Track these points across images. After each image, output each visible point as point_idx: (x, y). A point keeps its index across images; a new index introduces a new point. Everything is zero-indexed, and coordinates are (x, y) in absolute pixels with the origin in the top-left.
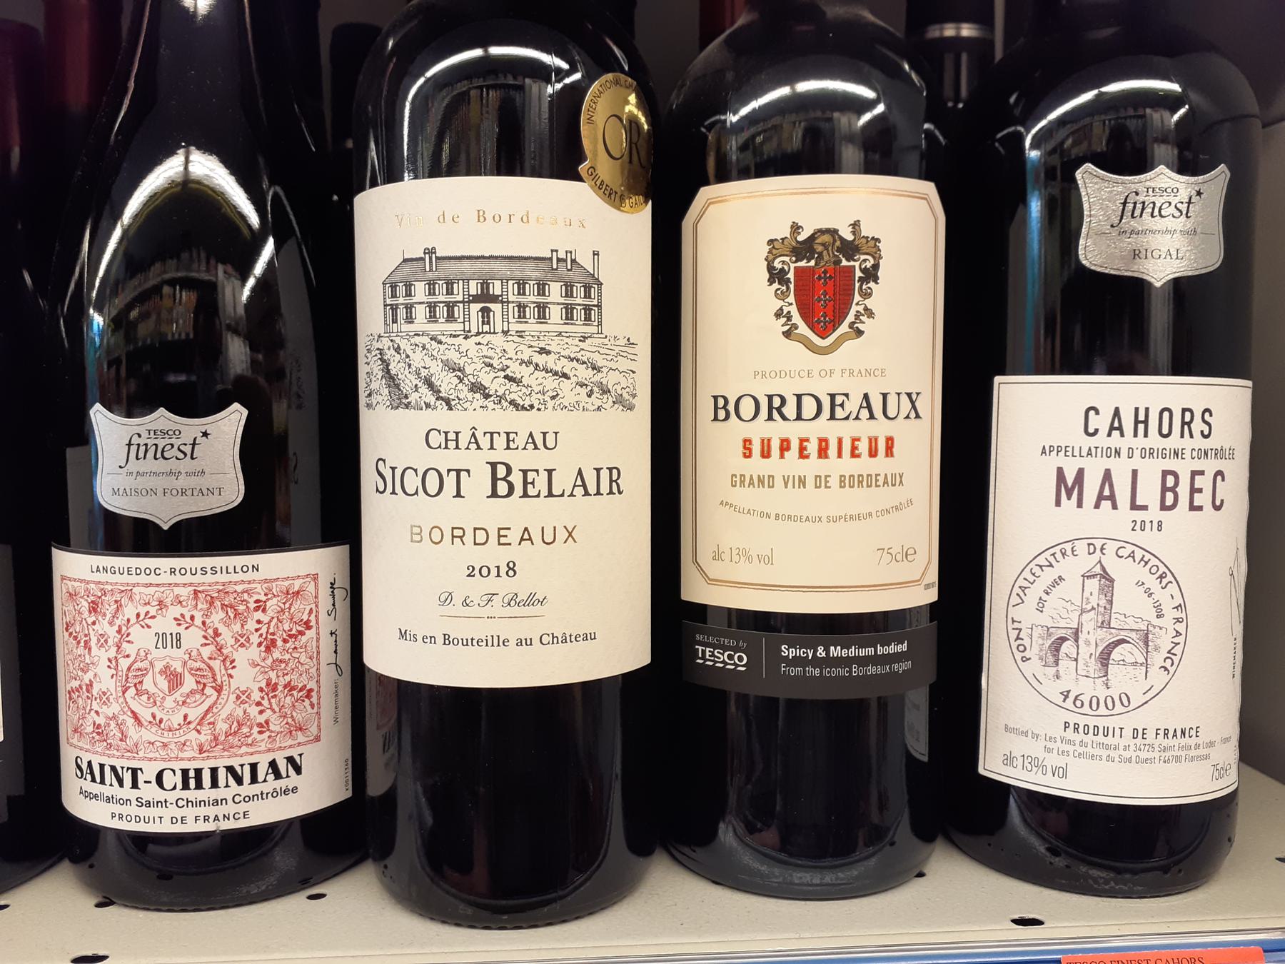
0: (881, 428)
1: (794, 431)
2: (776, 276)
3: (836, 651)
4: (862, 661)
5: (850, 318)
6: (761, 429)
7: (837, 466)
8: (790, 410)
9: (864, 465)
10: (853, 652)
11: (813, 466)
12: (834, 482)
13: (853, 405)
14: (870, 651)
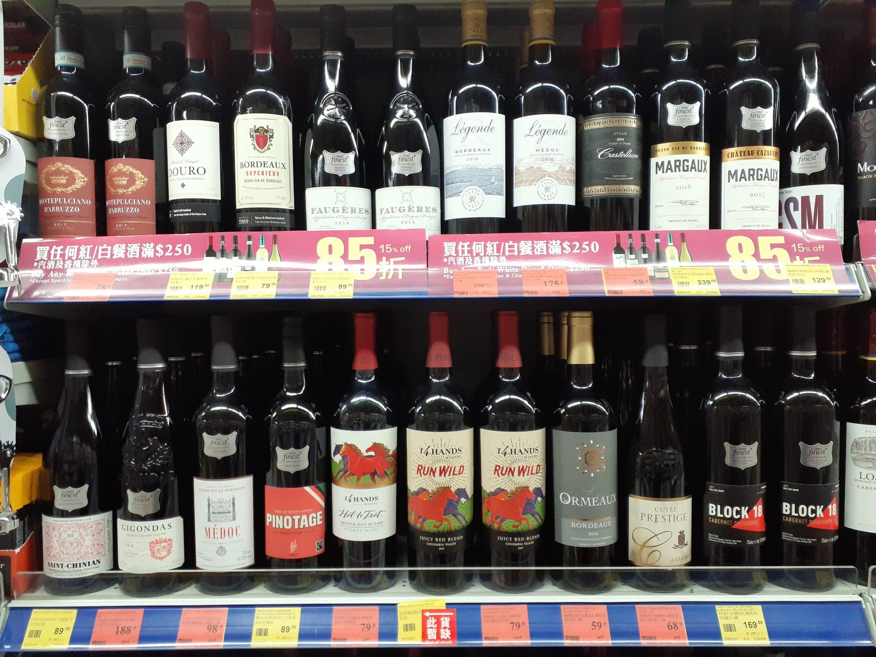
0: (275, 170)
1: (256, 169)
2: (252, 136)
3: (267, 218)
4: (273, 220)
5: (267, 146)
6: (250, 169)
7: (265, 177)
8: (255, 165)
9: (272, 177)
10: (270, 218)
11: (261, 177)
12: (265, 181)
13: (269, 164)
14: (275, 218)
